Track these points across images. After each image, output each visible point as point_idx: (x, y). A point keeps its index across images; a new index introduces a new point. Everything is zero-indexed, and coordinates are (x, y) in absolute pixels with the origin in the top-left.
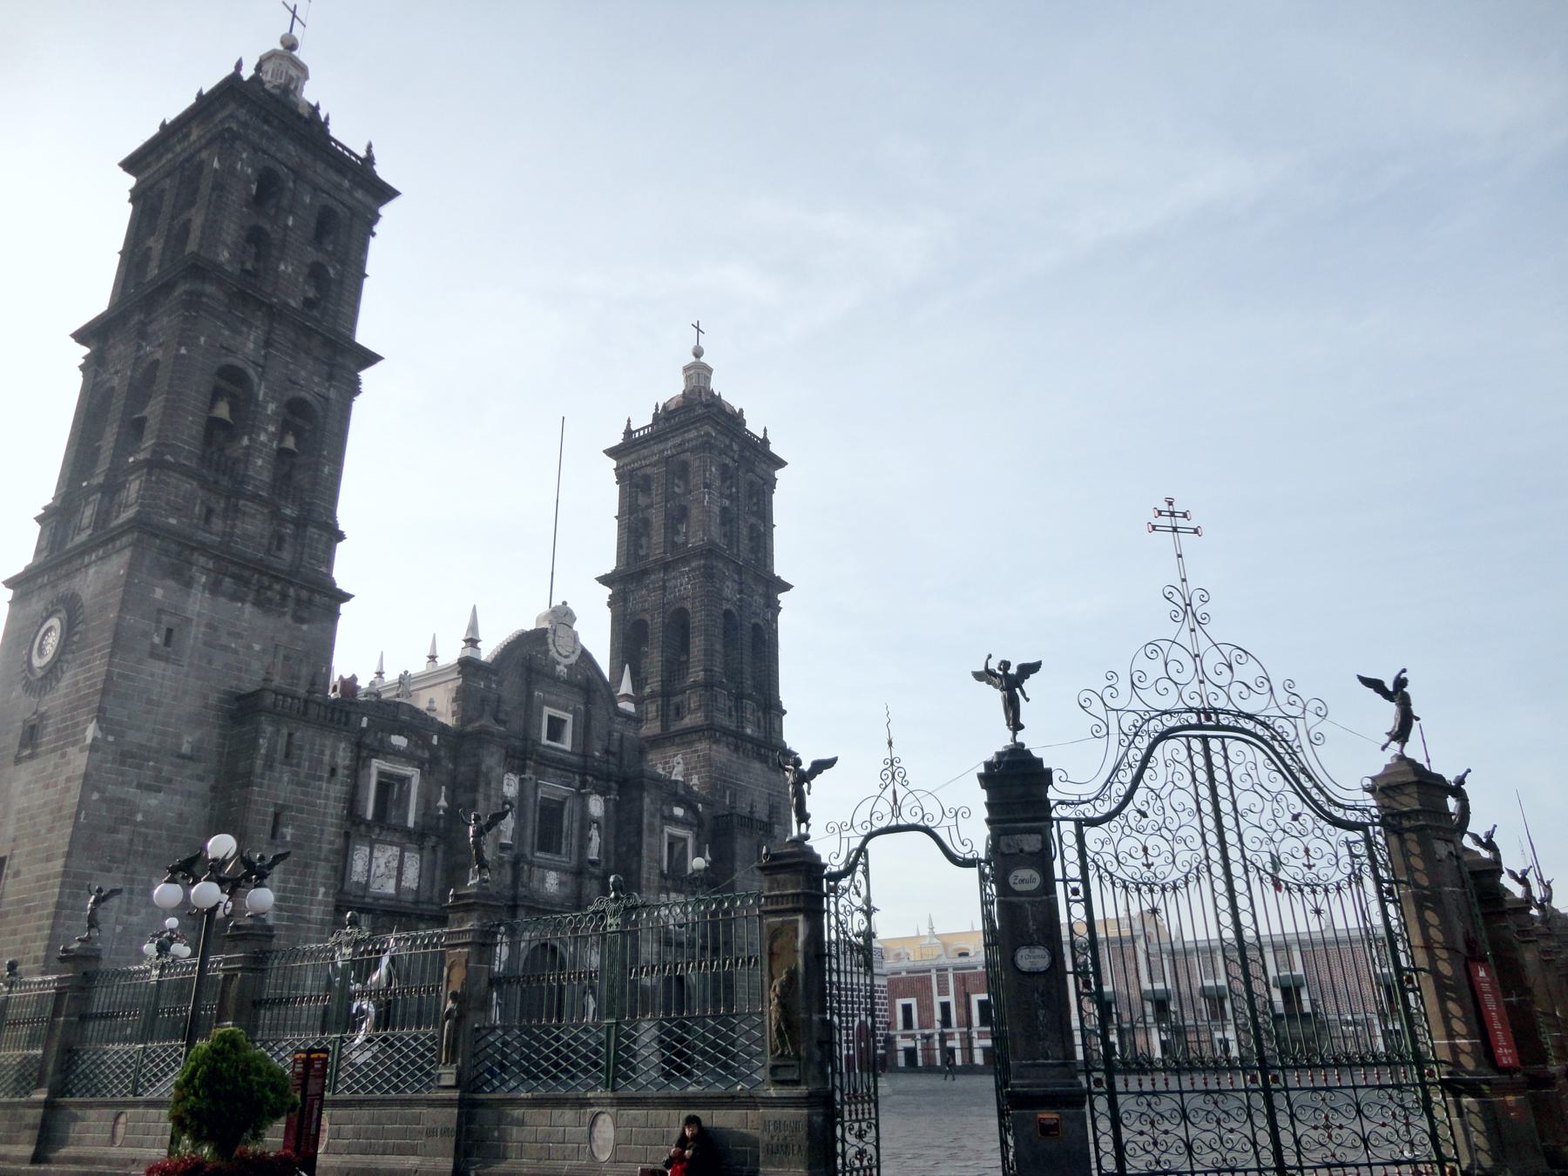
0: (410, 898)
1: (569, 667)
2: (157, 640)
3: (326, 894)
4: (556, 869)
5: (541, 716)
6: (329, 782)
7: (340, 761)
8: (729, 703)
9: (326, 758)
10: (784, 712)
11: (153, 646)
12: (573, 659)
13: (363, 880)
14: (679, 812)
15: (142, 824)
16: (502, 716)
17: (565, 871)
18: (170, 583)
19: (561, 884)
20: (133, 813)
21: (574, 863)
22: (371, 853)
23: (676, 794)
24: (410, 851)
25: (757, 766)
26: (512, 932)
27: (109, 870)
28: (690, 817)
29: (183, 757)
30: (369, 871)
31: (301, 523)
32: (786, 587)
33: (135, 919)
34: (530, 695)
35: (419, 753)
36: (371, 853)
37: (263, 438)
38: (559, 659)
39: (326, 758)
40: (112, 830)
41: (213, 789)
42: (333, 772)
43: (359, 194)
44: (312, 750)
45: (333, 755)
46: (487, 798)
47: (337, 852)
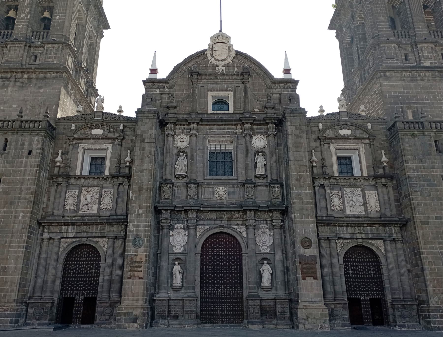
0: (108, 214)
1: (227, 65)
3: (23, 217)
4: (224, 185)
5: (206, 97)
6: (27, 158)
7: (34, 147)
9: (26, 146)
14: (346, 132)
16: (174, 104)
17: (234, 185)
19: (229, 193)
21: (242, 179)
22: (80, 192)
23: (339, 120)
24: (107, 188)
26: (187, 228)
28: (358, 133)
30: (78, 202)
31: (42, 45)
35: (111, 135)
36: (80, 192)
38: (217, 63)
39: (26, 146)
42: (30, 153)
44: (17, 144)
46: (143, 149)
47: (32, 193)
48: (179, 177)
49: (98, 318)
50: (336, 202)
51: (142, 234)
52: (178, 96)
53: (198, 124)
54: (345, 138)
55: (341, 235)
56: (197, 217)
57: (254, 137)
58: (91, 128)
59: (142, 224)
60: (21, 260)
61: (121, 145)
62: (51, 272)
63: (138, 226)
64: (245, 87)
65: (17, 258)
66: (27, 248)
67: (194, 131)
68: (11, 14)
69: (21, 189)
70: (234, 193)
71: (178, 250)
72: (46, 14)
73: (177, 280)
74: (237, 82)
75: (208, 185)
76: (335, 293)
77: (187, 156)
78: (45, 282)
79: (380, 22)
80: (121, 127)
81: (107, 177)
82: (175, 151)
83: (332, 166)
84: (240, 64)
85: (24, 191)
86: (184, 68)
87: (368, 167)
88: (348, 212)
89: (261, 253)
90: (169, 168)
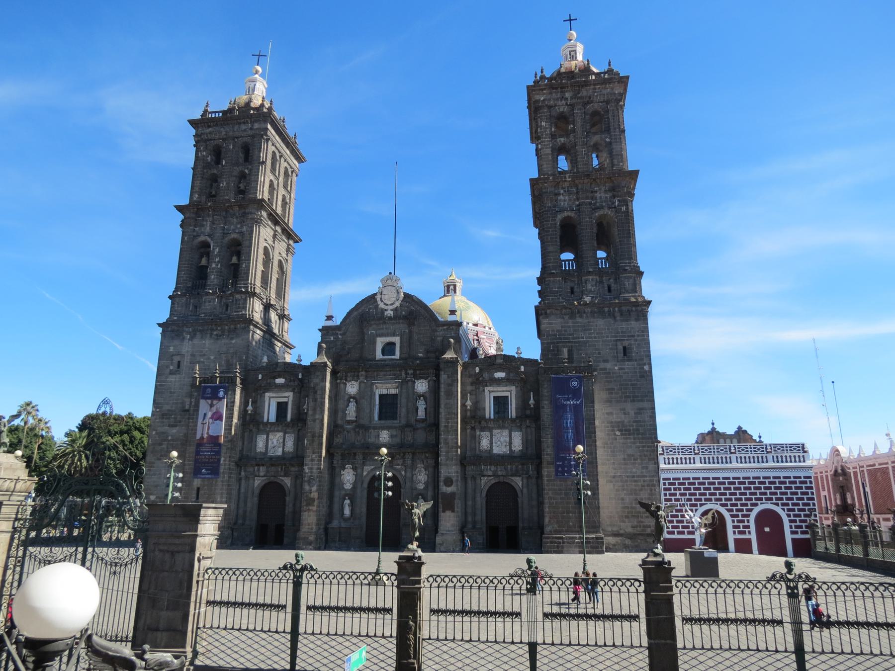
1: (395, 310)
2: (171, 368)
5: (375, 343)
8: (570, 284)
10: (642, 273)
11: (171, 370)
12: (398, 304)
13: (263, 450)
14: (500, 375)
15: (172, 440)
17: (395, 428)
18: (176, 342)
19: (392, 436)
21: (403, 422)
24: (289, 433)
25: (600, 323)
26: (354, 469)
32: (634, 174)
34: (362, 334)
35: (292, 383)
37: (214, 265)
38: (386, 307)
40: (161, 444)
43: (256, 126)
48: (349, 422)
49: (286, 540)
50: (485, 443)
52: (350, 340)
53: (366, 371)
54: (499, 382)
55: (485, 473)
56: (364, 458)
57: (417, 382)
58: (275, 378)
59: (315, 467)
60: (225, 496)
61: (300, 393)
62: (249, 504)
63: (311, 469)
64: (410, 332)
65: (222, 494)
66: (229, 485)
67: (362, 379)
68: (204, 262)
70: (396, 436)
71: (348, 486)
72: (234, 260)
73: (347, 512)
74: (403, 327)
75: (375, 428)
76: (474, 523)
77: (356, 402)
78: (245, 512)
79: (549, 252)
80: (300, 376)
81: (289, 423)
82: (347, 397)
83: (484, 409)
84: (408, 307)
86: (355, 313)
87: (517, 409)
88: (495, 452)
89: (416, 488)
90: (340, 414)
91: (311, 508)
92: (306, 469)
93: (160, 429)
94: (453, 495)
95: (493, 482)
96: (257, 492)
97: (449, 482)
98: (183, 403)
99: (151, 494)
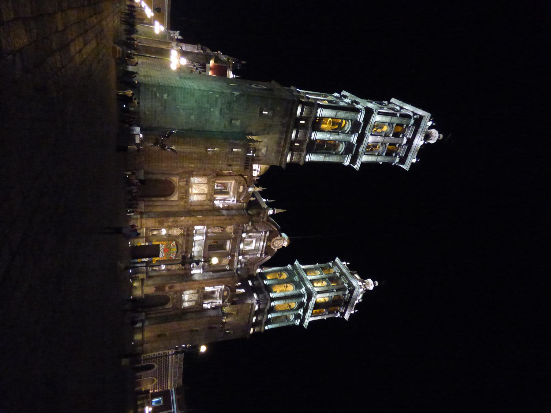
1: (270, 246)
2: (265, 109)
3: (192, 167)
12: (272, 247)
20: (213, 108)
22: (205, 183)
27: (196, 102)
29: (231, 121)
30: (199, 183)
33: (181, 111)
36: (205, 183)
39: (235, 163)
40: (208, 102)
41: (222, 132)
45: (235, 165)
51: (179, 224)
58: (244, 186)
59: (183, 223)
69: (208, 163)
82: (225, 226)
85: (206, 166)
91: (157, 225)
92: (183, 218)
93: (219, 101)
94: (164, 290)
95: (170, 297)
96: (168, 179)
97: (171, 288)
98: (237, 120)
99: (168, 96)
